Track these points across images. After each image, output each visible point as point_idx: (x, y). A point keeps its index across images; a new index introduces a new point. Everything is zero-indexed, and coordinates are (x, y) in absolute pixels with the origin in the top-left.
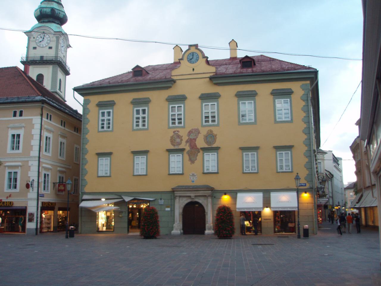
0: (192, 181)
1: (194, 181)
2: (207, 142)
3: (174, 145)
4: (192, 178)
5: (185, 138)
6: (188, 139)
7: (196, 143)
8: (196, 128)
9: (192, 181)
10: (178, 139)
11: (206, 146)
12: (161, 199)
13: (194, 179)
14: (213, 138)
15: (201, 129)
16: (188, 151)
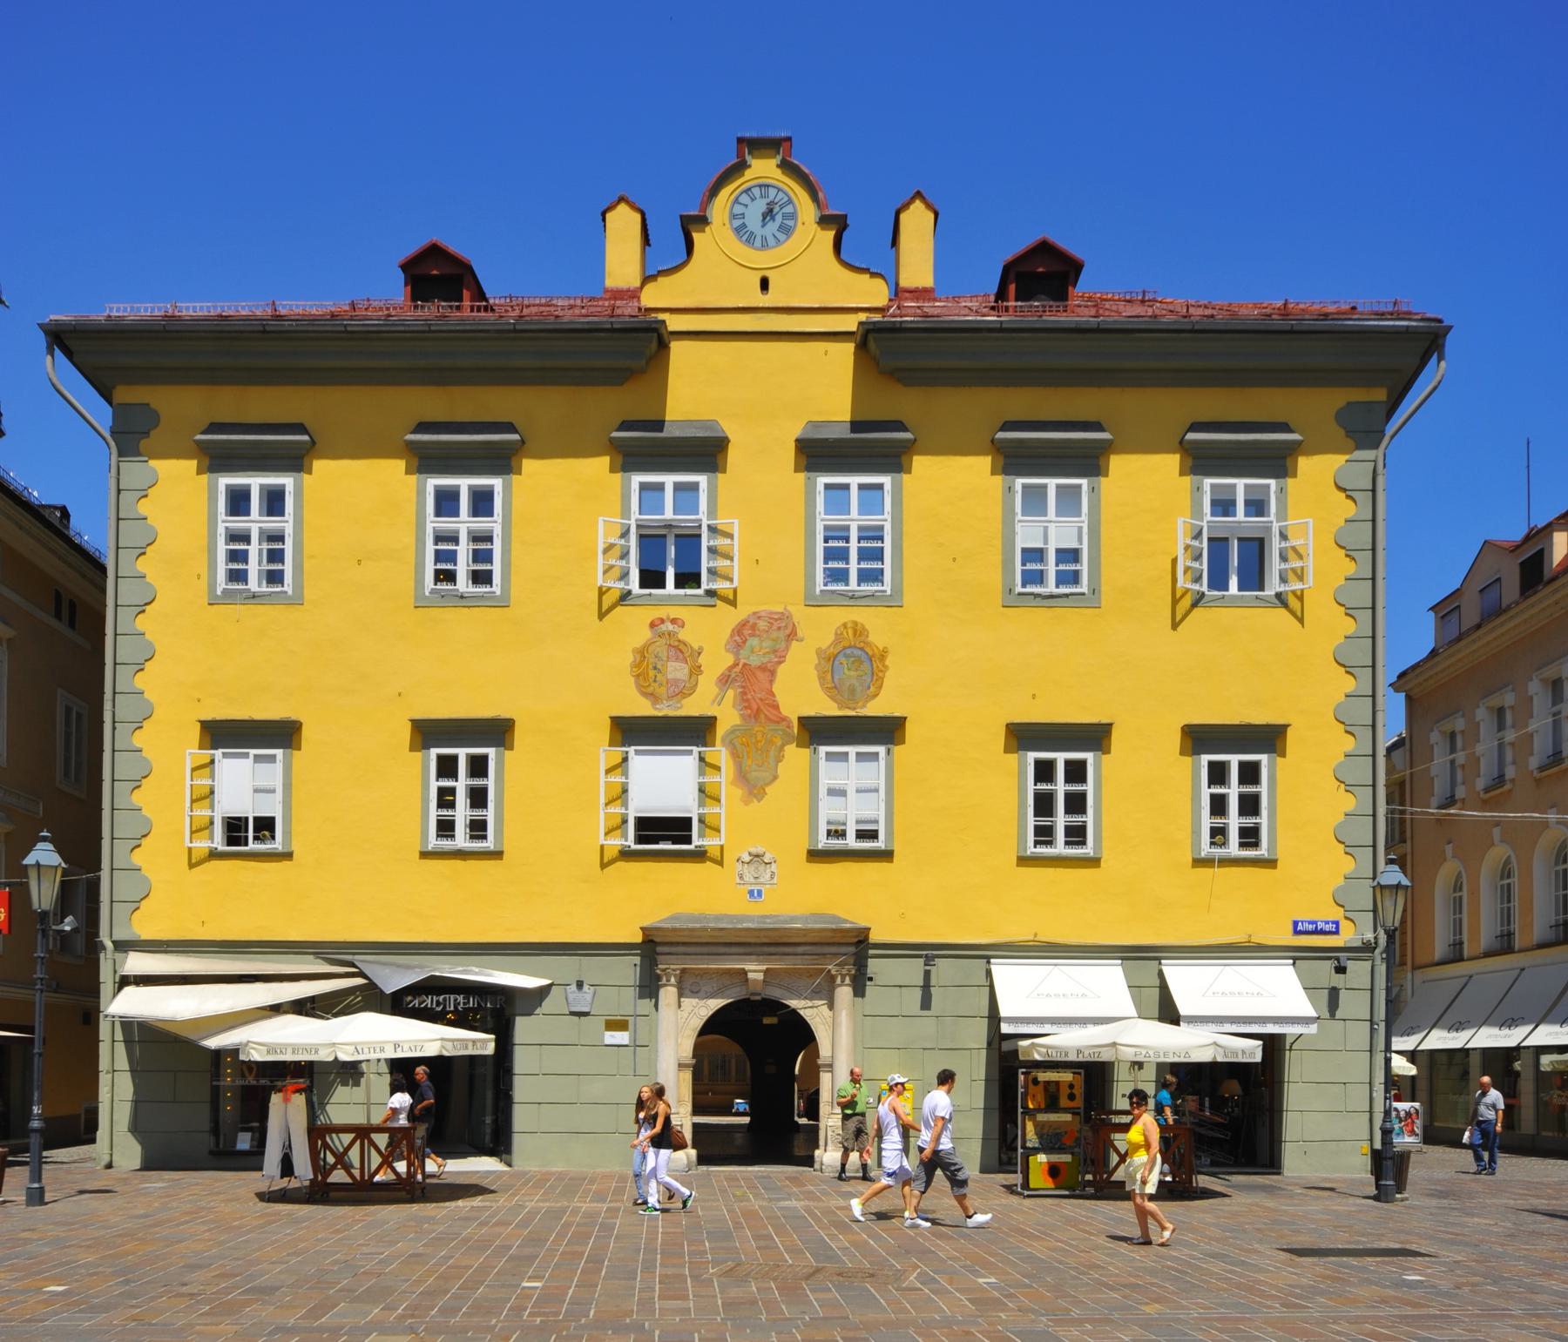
0: (751, 893)
1: (760, 893)
2: (834, 689)
3: (654, 698)
4: (748, 878)
5: (717, 660)
6: (730, 669)
7: (776, 688)
8: (780, 609)
9: (751, 893)
10: (677, 665)
11: (831, 709)
14: (866, 666)
15: (799, 613)
16: (733, 731)
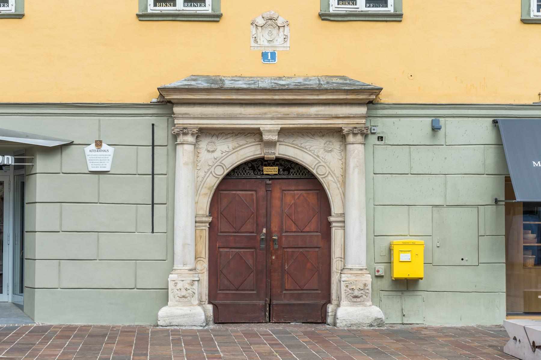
0: (264, 55)
1: (273, 54)
4: (263, 41)
12: (99, 144)
13: (276, 43)
